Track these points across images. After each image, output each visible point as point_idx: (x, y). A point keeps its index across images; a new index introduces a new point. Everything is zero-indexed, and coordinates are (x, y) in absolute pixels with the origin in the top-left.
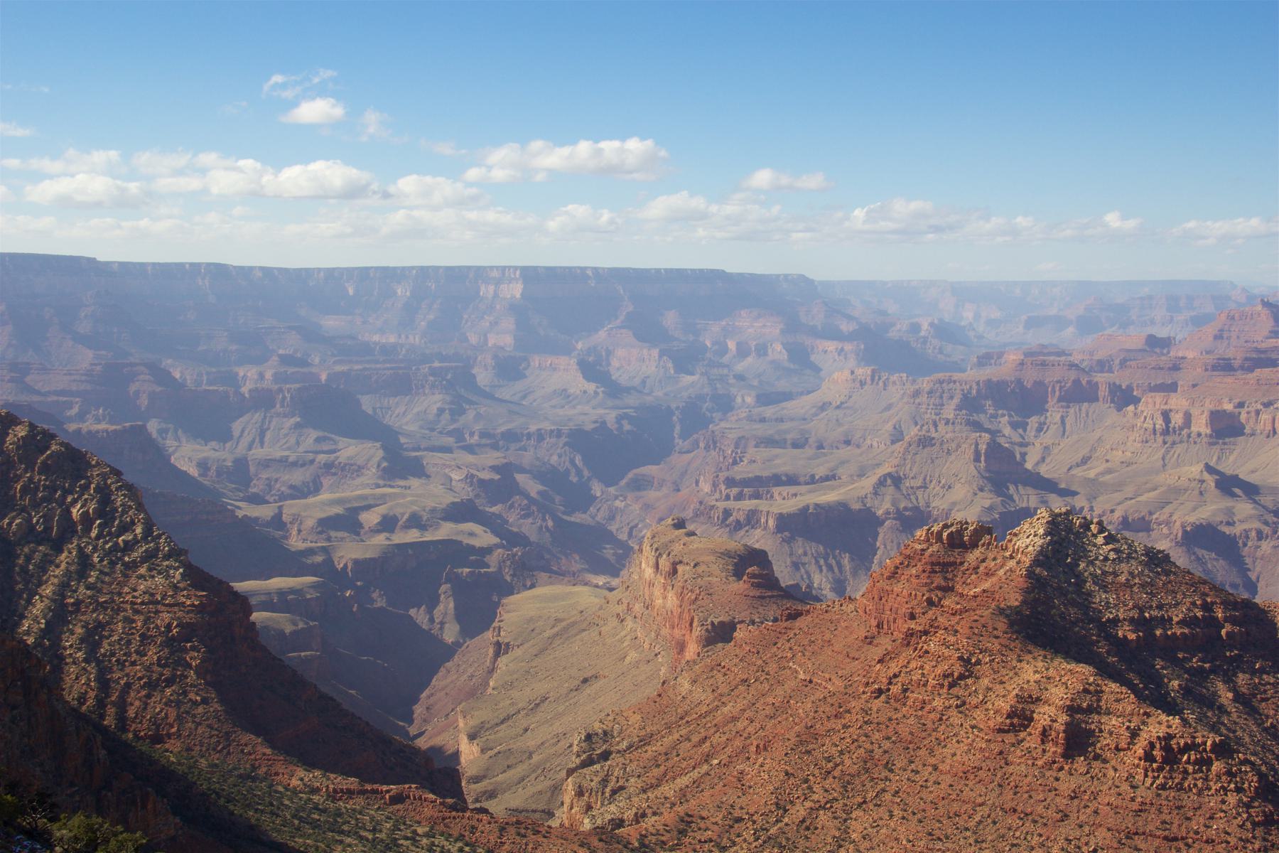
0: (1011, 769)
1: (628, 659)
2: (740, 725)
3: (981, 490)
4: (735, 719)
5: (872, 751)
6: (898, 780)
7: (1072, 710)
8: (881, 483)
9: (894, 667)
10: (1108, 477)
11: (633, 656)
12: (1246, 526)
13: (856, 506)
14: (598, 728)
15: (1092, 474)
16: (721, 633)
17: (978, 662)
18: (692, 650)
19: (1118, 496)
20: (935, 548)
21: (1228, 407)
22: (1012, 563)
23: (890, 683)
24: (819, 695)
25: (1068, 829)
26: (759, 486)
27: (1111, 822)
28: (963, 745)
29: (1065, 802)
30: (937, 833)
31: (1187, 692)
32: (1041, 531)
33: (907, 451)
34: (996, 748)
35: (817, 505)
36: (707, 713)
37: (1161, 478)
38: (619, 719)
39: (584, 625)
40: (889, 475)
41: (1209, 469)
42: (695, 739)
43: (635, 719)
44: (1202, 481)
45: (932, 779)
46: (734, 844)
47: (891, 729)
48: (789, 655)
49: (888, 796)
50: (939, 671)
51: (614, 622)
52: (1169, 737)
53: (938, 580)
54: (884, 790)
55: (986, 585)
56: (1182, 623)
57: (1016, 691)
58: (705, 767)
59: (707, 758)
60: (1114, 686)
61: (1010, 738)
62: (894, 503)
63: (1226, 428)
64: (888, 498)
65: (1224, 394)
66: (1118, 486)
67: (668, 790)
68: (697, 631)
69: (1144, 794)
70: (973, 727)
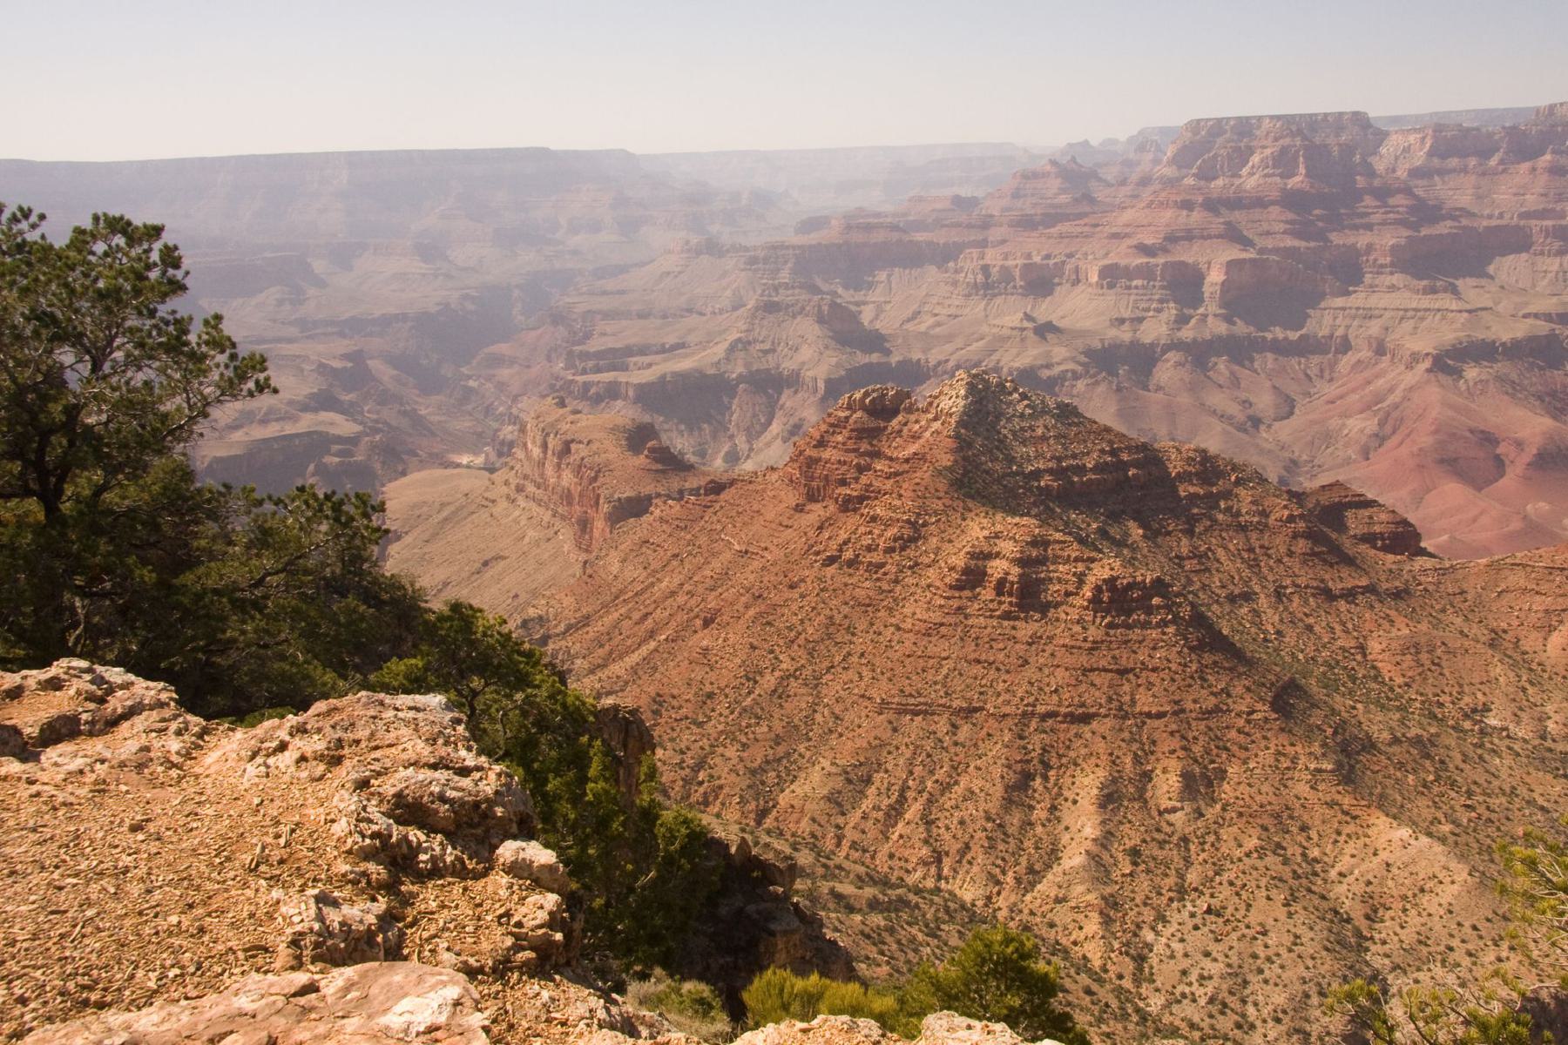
0: (970, 622)
1: (527, 540)
2: (681, 599)
3: (827, 347)
4: (673, 594)
5: (831, 618)
6: (861, 642)
7: (1022, 562)
8: (732, 349)
9: (843, 536)
10: (938, 330)
11: (531, 534)
12: (1062, 368)
13: (712, 371)
14: (532, 612)
15: (923, 328)
16: (635, 507)
17: (925, 525)
18: (599, 524)
19: (949, 348)
20: (859, 414)
21: (1037, 259)
22: (937, 425)
23: (841, 550)
24: (756, 564)
25: (1030, 672)
26: (616, 359)
27: (1069, 660)
28: (920, 605)
29: (1025, 647)
30: (908, 690)
31: (1103, 533)
32: (963, 392)
33: (754, 316)
34: (955, 603)
35: (674, 374)
36: (643, 591)
37: (985, 329)
38: (553, 602)
39: (473, 507)
40: (739, 340)
41: (1028, 317)
42: (636, 616)
43: (569, 601)
44: (1023, 329)
45: (896, 638)
46: (710, 718)
47: (848, 593)
48: (719, 527)
49: (855, 659)
50: (889, 534)
51: (503, 504)
52: (1113, 580)
53: (864, 447)
54: (849, 654)
55: (912, 448)
56: (1095, 469)
57: (968, 549)
58: (653, 644)
59: (652, 634)
60: (1058, 536)
61: (967, 593)
62: (746, 365)
63: (1040, 283)
64: (740, 362)
65: (1036, 248)
66: (949, 338)
67: (618, 668)
68: (605, 508)
69: (1094, 633)
70: (929, 586)
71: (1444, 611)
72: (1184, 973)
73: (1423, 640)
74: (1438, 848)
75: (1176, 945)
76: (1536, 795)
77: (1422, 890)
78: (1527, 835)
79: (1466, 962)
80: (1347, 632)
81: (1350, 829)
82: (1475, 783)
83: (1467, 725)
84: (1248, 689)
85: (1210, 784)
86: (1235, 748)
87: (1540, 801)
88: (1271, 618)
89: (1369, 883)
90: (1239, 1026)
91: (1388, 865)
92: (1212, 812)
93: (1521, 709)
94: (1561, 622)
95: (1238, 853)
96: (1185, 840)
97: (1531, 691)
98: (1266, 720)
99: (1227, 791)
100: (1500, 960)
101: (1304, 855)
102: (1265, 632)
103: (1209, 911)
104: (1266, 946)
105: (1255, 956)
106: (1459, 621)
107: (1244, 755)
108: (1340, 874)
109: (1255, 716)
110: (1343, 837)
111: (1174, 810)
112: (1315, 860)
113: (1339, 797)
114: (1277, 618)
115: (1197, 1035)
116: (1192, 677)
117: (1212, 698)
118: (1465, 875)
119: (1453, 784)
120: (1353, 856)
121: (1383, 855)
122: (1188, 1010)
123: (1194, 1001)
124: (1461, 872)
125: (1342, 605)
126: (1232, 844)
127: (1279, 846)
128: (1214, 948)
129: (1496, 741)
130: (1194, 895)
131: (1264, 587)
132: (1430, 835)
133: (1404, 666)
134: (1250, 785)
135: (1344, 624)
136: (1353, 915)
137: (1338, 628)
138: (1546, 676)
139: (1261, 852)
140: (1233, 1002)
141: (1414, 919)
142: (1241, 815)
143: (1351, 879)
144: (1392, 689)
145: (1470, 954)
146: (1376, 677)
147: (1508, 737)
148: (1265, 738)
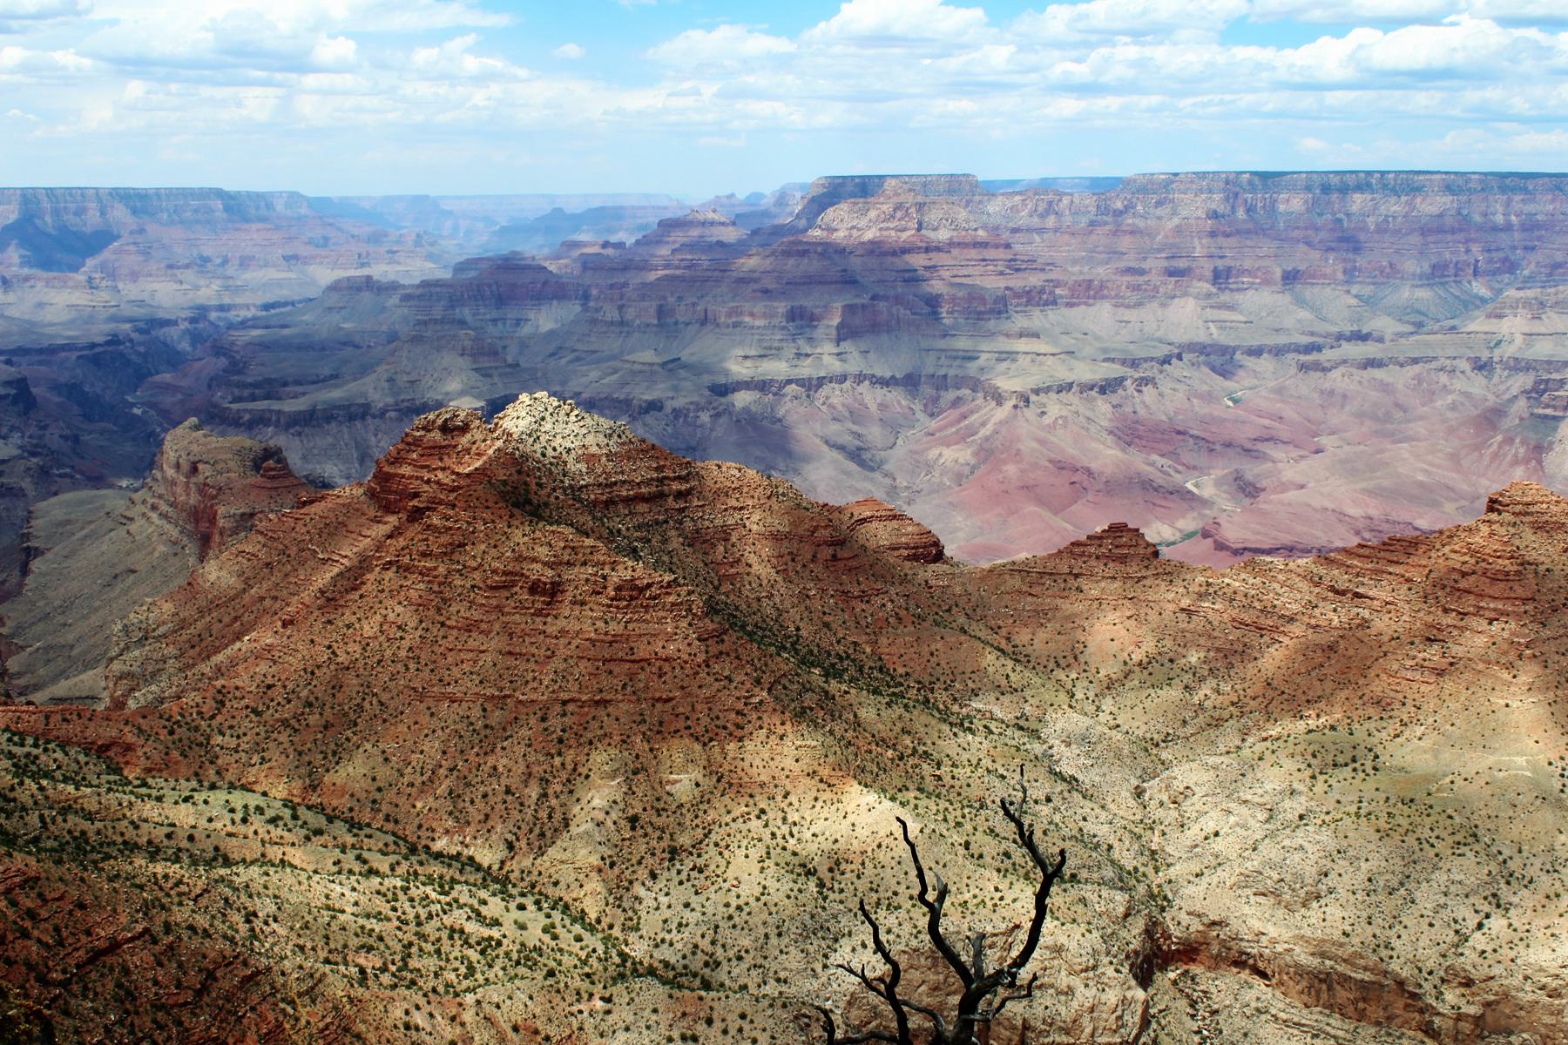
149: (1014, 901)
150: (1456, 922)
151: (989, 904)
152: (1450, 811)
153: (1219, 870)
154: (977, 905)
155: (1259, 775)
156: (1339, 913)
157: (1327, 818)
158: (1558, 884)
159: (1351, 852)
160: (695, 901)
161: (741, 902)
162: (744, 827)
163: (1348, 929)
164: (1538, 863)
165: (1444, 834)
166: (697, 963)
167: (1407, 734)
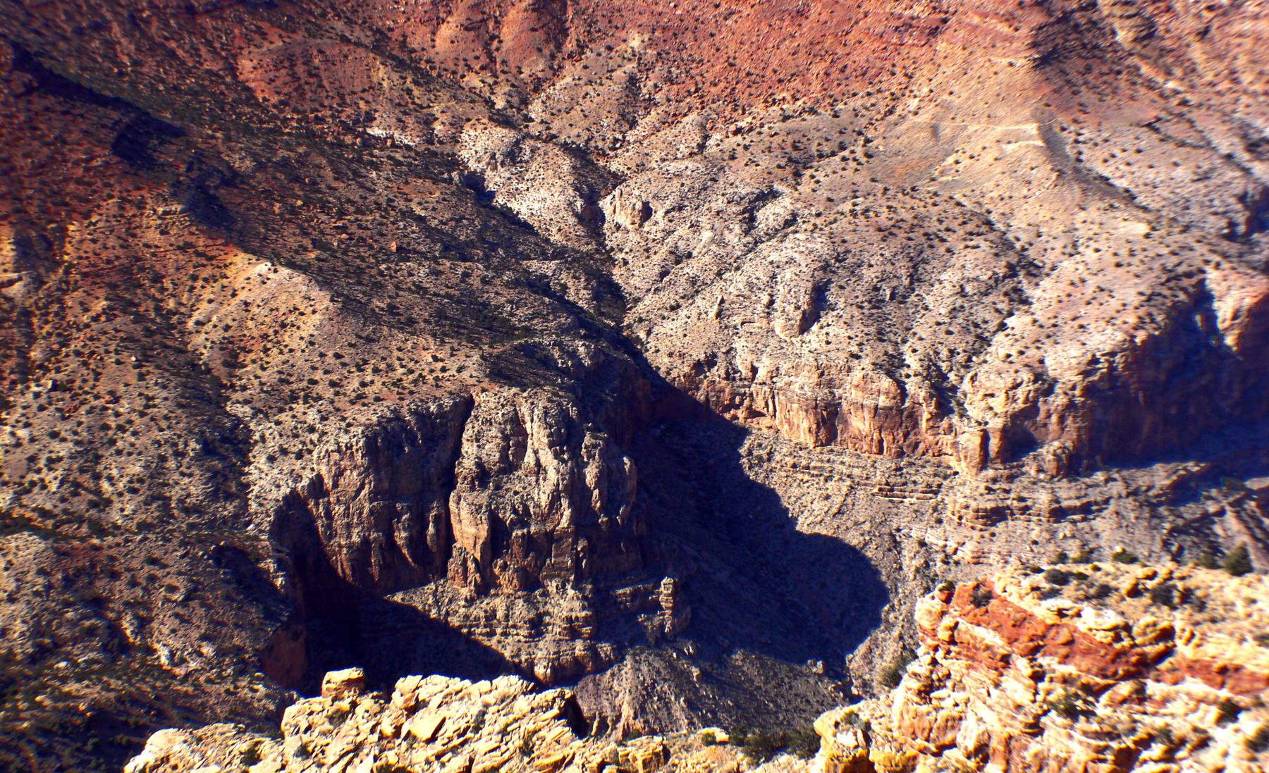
71: (324, 15)
72: (33, 459)
73: (298, 51)
74: (299, 278)
75: (23, 433)
76: (414, 206)
77: (283, 326)
78: (399, 249)
79: (329, 393)
80: (215, 52)
81: (205, 273)
82: (349, 201)
83: (348, 139)
84: (86, 133)
85: (50, 245)
86: (75, 203)
87: (419, 211)
88: (126, 46)
89: (227, 328)
90: (93, 505)
91: (246, 304)
92: (53, 280)
93: (405, 113)
94: (450, 13)
95: (85, 319)
96: (27, 314)
97: (416, 93)
98: (107, 165)
99: (70, 253)
100: (364, 385)
101: (158, 310)
102: (120, 65)
103: (55, 387)
104: (117, 414)
105: (106, 427)
106: (339, 25)
107: (85, 207)
108: (198, 323)
109: (94, 163)
110: (200, 283)
111: (11, 283)
112: (172, 313)
113: (192, 239)
114: (133, 47)
115: (50, 523)
116: (21, 129)
117: (45, 150)
118: (327, 302)
119: (324, 207)
120: (210, 301)
121: (242, 295)
122: (38, 499)
123: (44, 487)
124: (323, 300)
125: (208, 22)
126: (78, 310)
127: (132, 304)
128: (64, 428)
129: (376, 152)
130: (39, 372)
131: (116, 14)
132: (291, 265)
133: (278, 83)
134: (94, 241)
135: (209, 44)
136: (212, 365)
137: (203, 51)
138: (434, 74)
139: (109, 313)
140: (86, 480)
141: (275, 358)
142: (85, 275)
143: (209, 327)
144: (265, 110)
145: (333, 384)
146: (248, 99)
147: (393, 145)
148: (108, 185)
149: (460, 370)
150: (976, 326)
151: (430, 379)
152: (958, 197)
153: (698, 299)
154: (415, 382)
155: (732, 178)
156: (843, 333)
157: (818, 221)
158: (1081, 267)
159: (850, 260)
160: (60, 427)
161: (121, 421)
162: (109, 327)
163: (855, 349)
164: (1058, 245)
165: (954, 225)
166: (80, 504)
167: (899, 111)
